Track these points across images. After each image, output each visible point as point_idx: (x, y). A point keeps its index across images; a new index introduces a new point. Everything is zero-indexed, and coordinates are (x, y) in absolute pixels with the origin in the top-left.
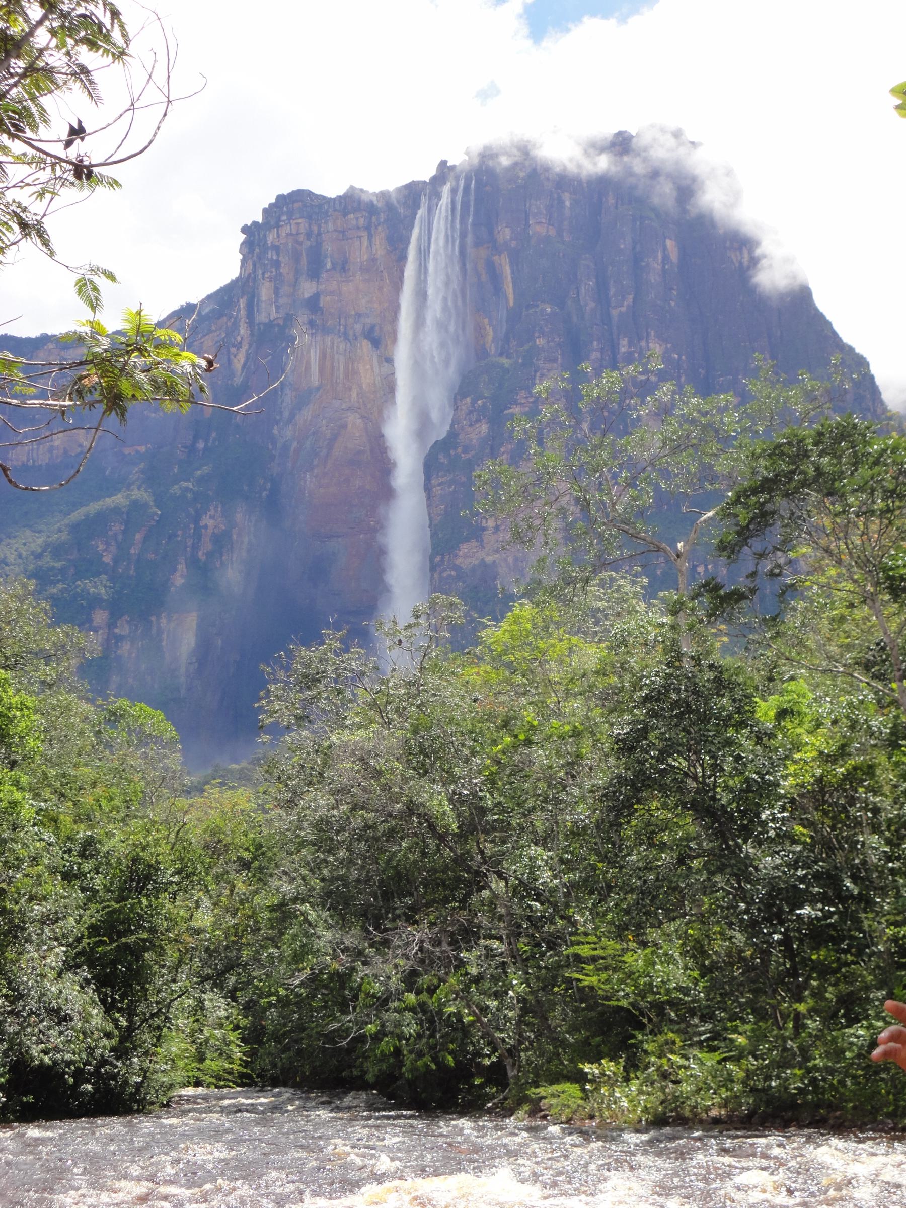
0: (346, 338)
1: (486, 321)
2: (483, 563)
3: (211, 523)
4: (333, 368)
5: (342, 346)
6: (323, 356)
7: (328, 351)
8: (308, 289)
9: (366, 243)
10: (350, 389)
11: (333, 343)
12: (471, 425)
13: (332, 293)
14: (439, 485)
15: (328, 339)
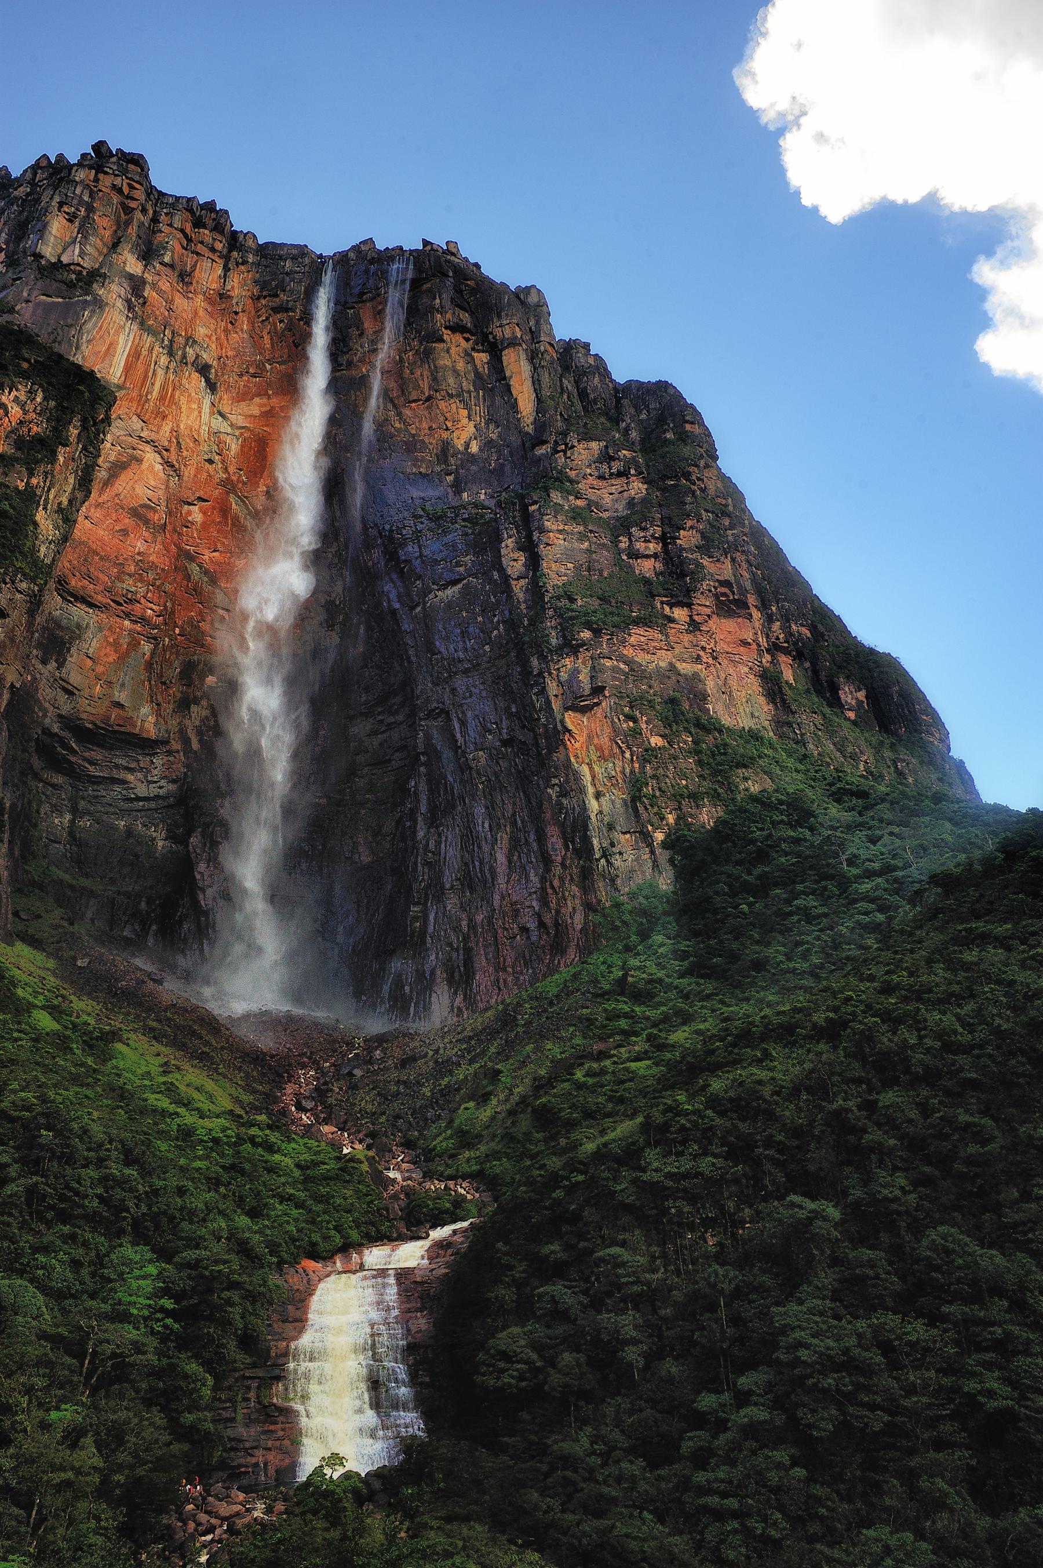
0: (171, 354)
1: (465, 413)
2: (672, 667)
3: (15, 411)
4: (146, 376)
5: (164, 360)
6: (135, 354)
7: (144, 353)
8: (133, 265)
9: (220, 272)
10: (164, 417)
11: (151, 350)
12: (601, 477)
13: (161, 293)
14: (560, 532)
15: (148, 340)
